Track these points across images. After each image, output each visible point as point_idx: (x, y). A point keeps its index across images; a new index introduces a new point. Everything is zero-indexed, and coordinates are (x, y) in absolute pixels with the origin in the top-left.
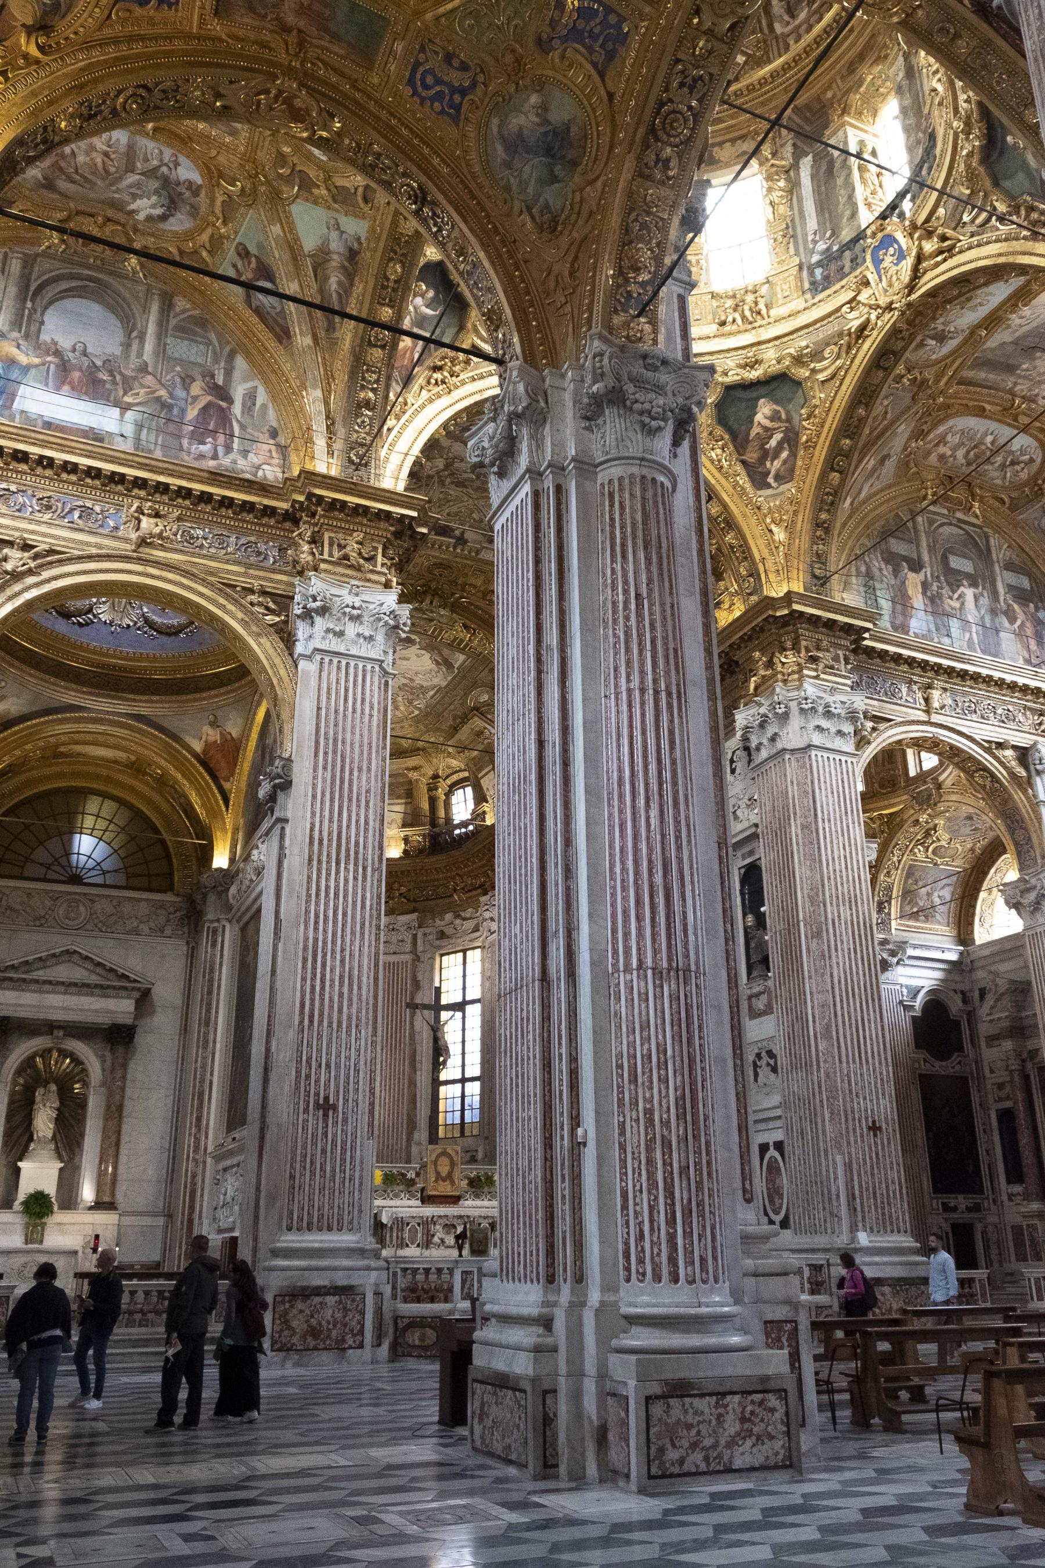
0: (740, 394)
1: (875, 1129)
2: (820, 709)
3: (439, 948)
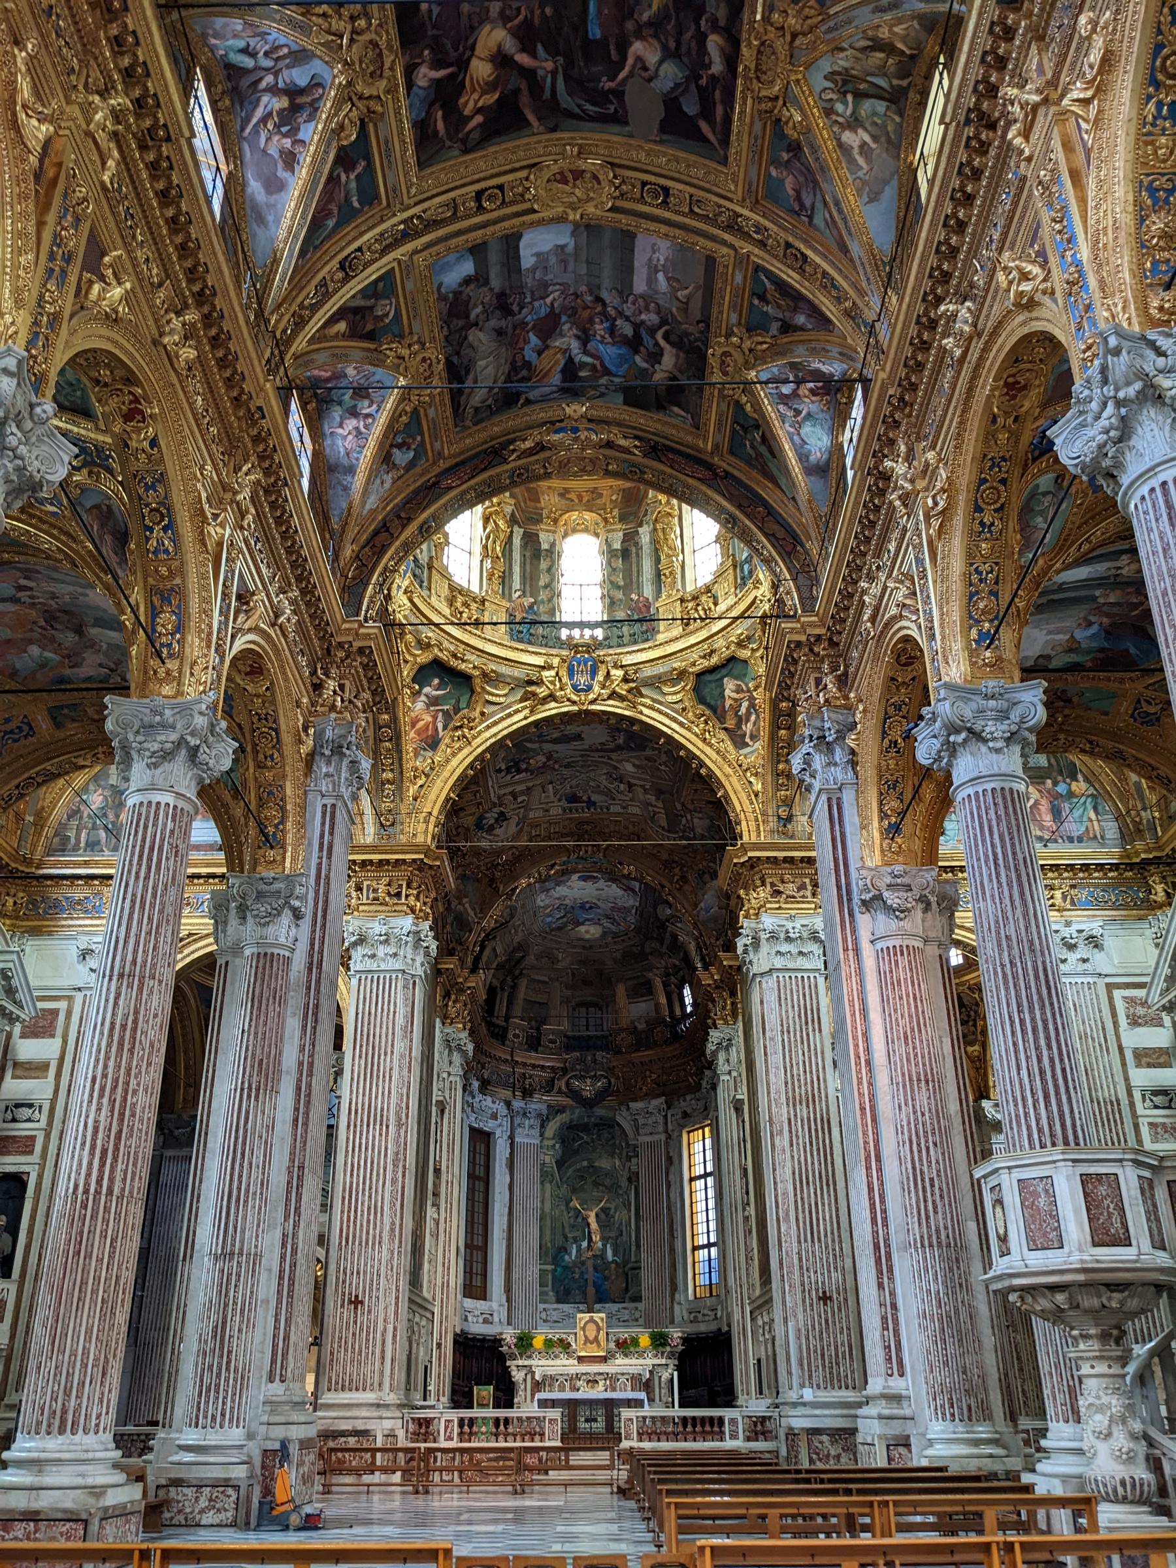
0: (708, 677)
1: (825, 1298)
2: (782, 936)
3: (683, 1127)
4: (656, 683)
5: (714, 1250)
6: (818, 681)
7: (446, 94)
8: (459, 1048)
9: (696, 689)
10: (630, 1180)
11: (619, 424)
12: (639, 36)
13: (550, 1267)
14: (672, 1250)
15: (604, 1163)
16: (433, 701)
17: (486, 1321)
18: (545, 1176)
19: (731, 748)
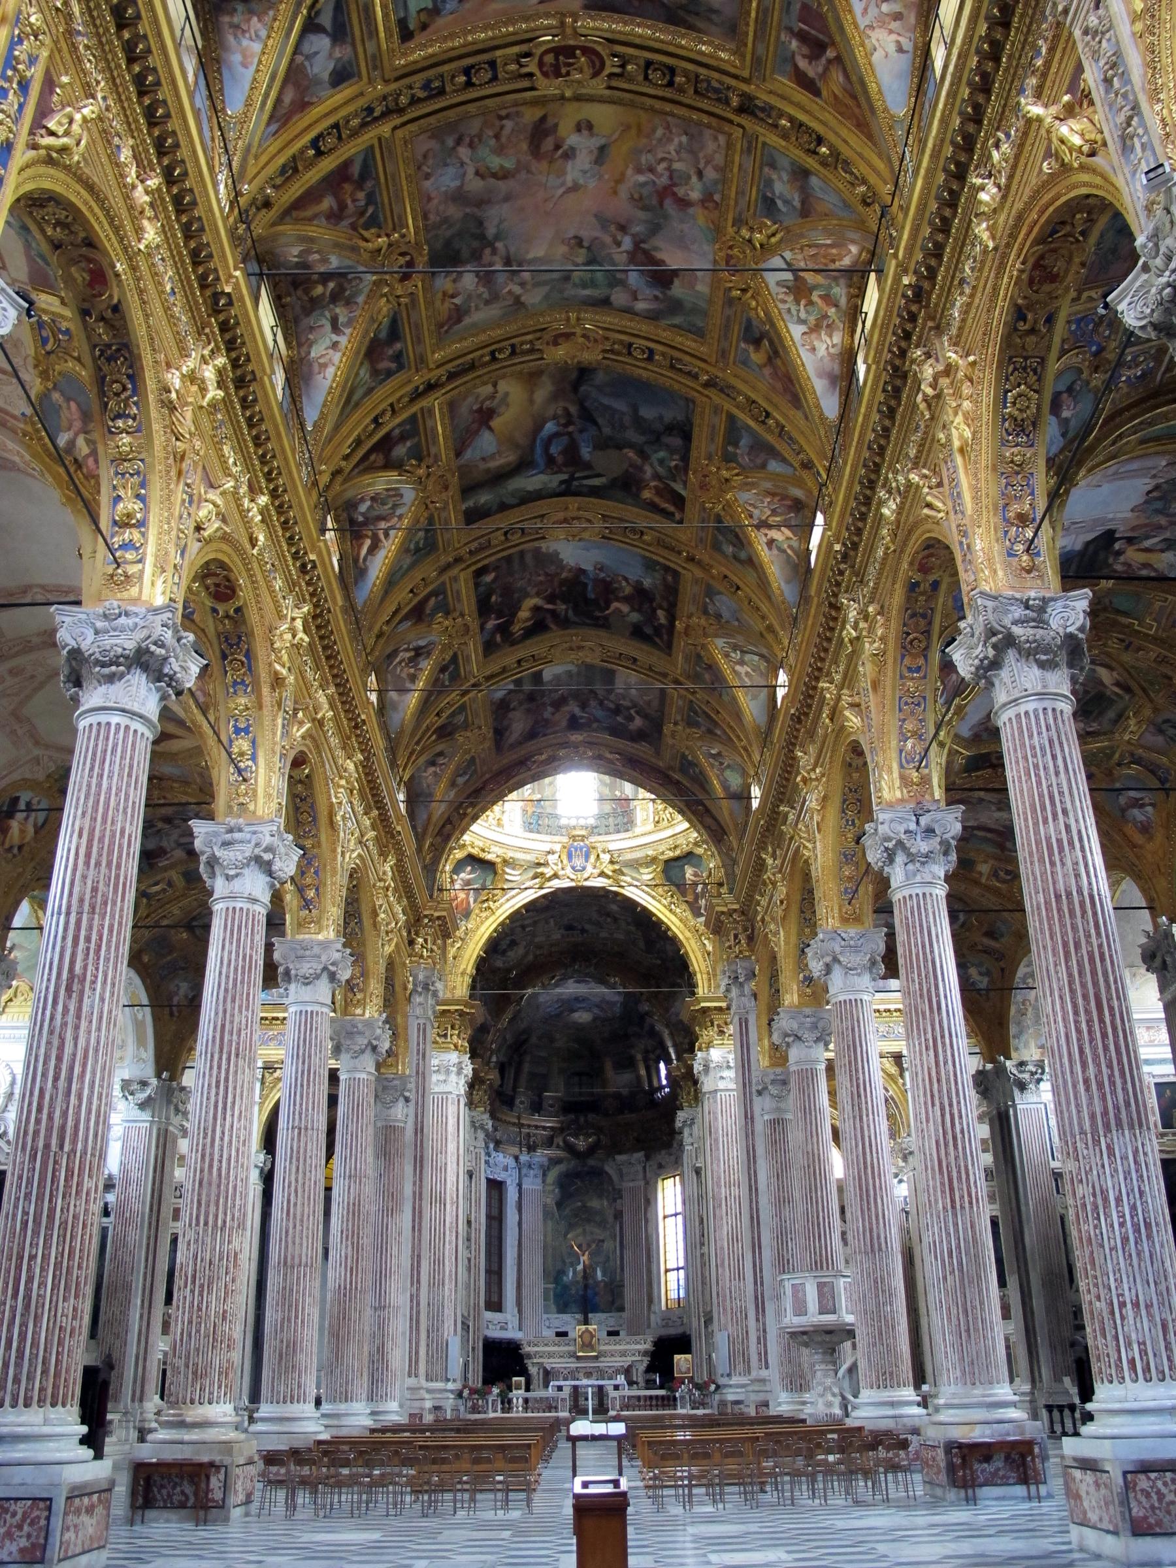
4: (636, 865)
5: (682, 1272)
6: (736, 936)
7: (503, 629)
8: (482, 1127)
9: (665, 871)
10: (616, 1217)
11: (607, 746)
12: (618, 599)
13: (552, 1286)
14: (649, 1272)
15: (595, 1203)
16: (468, 883)
17: (502, 1328)
18: (547, 1214)
19: (690, 917)
